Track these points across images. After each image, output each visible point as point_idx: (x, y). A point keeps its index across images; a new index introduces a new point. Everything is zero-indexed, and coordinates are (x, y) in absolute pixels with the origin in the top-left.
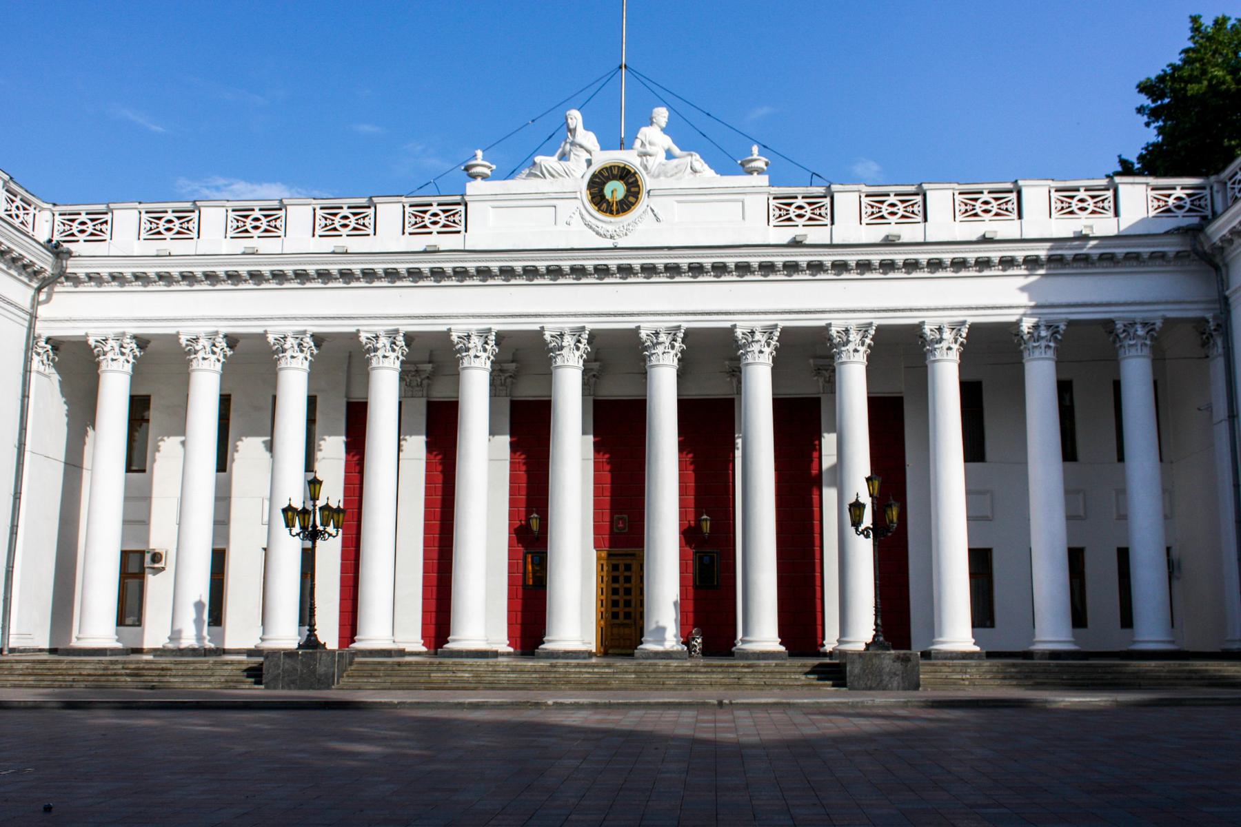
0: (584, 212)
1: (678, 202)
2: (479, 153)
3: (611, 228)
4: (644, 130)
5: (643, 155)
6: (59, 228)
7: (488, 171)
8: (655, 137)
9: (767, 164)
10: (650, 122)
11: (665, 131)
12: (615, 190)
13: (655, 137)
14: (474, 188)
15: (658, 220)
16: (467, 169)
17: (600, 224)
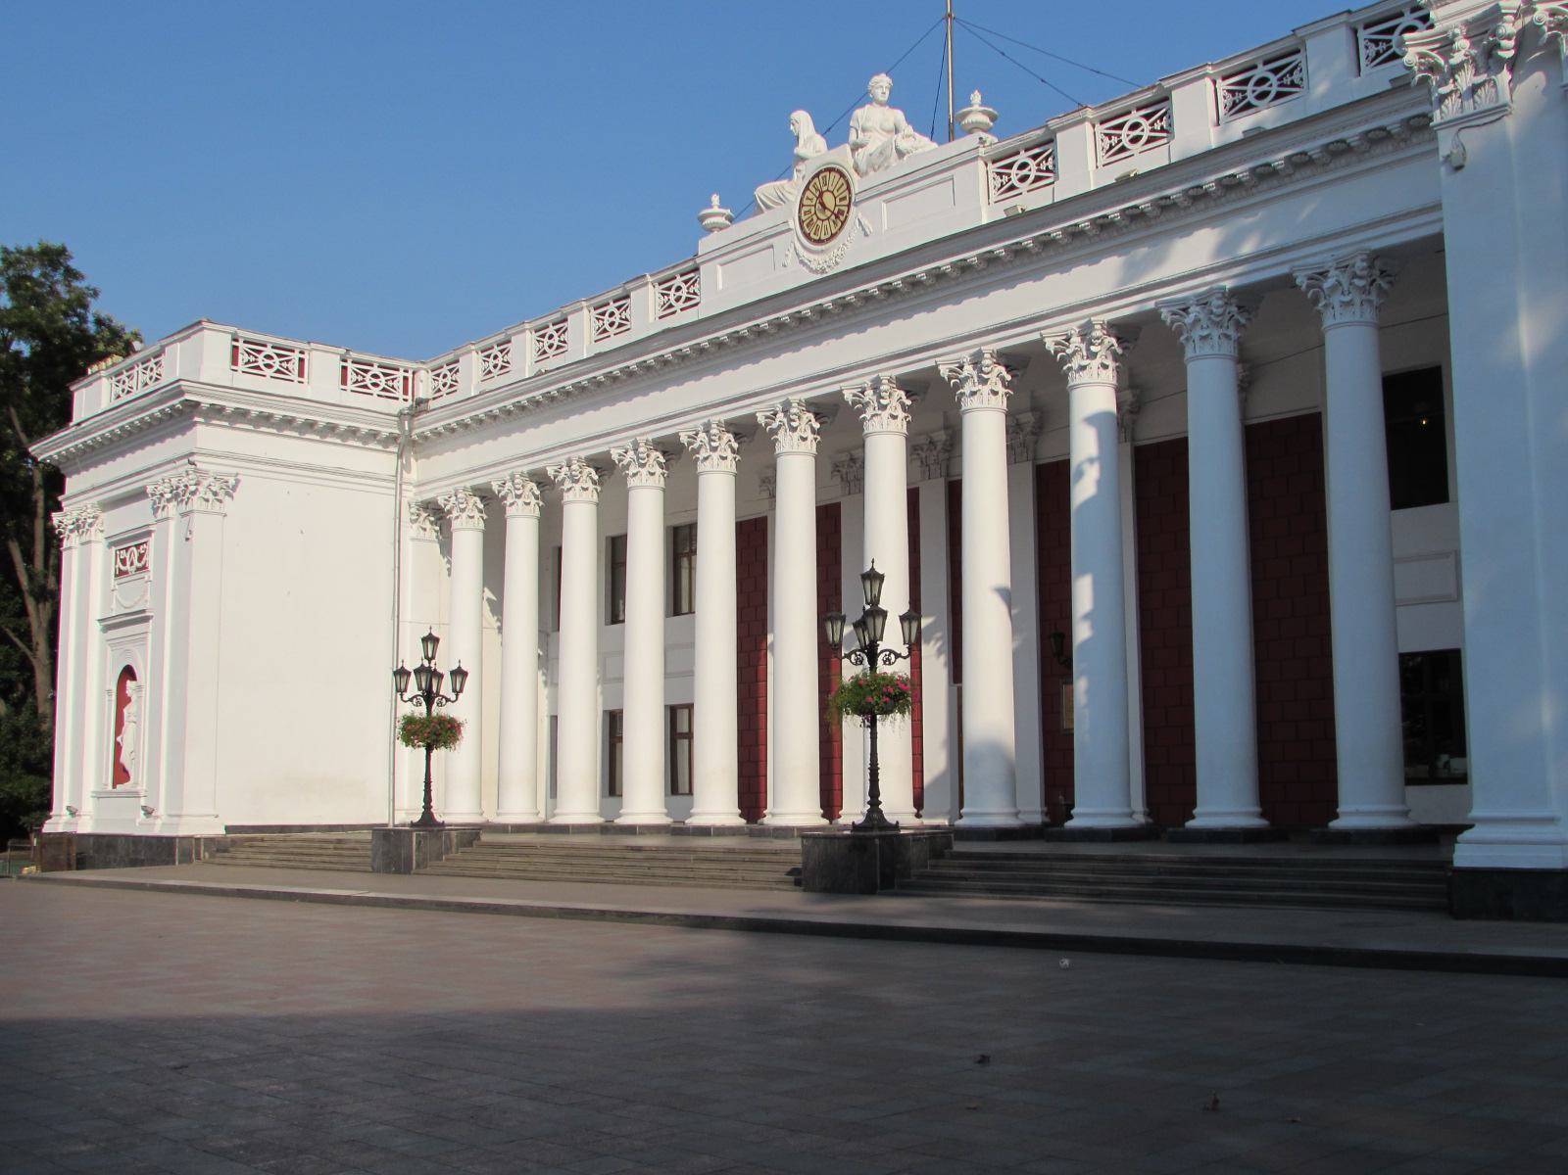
0: (798, 245)
1: (887, 201)
2: (715, 199)
3: (820, 258)
4: (858, 113)
5: (855, 148)
6: (431, 384)
7: (722, 220)
8: (879, 122)
9: (993, 118)
10: (865, 98)
11: (892, 102)
12: (828, 207)
13: (879, 122)
14: (705, 245)
15: (866, 235)
16: (702, 219)
17: (812, 257)
